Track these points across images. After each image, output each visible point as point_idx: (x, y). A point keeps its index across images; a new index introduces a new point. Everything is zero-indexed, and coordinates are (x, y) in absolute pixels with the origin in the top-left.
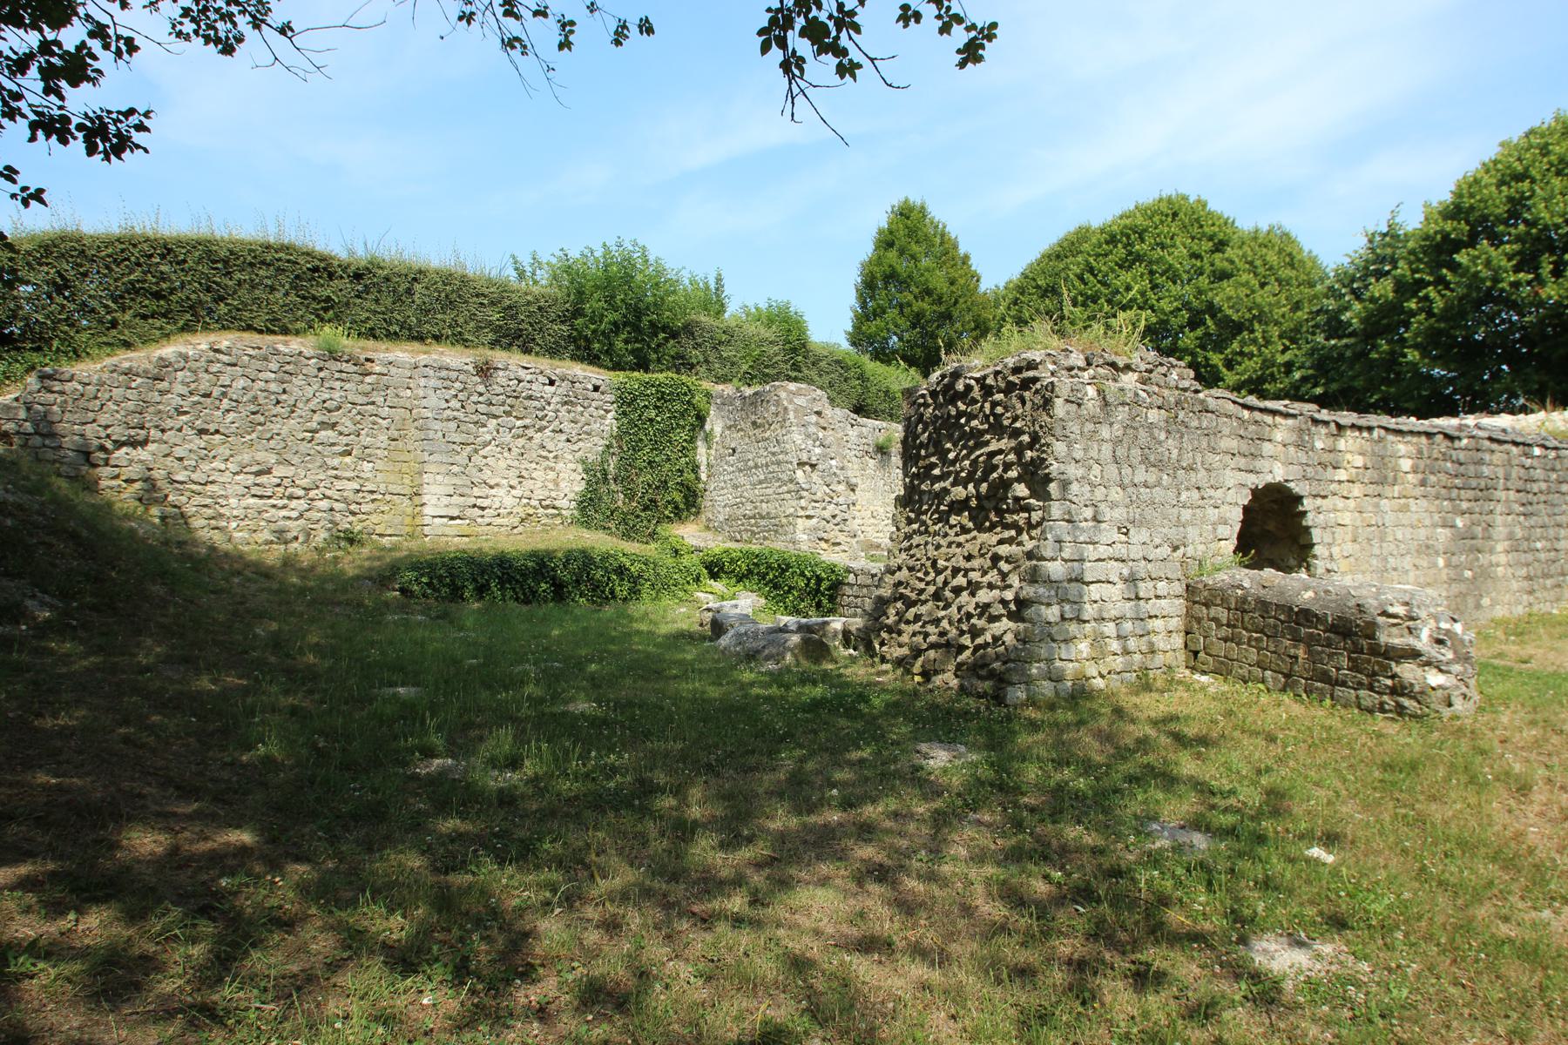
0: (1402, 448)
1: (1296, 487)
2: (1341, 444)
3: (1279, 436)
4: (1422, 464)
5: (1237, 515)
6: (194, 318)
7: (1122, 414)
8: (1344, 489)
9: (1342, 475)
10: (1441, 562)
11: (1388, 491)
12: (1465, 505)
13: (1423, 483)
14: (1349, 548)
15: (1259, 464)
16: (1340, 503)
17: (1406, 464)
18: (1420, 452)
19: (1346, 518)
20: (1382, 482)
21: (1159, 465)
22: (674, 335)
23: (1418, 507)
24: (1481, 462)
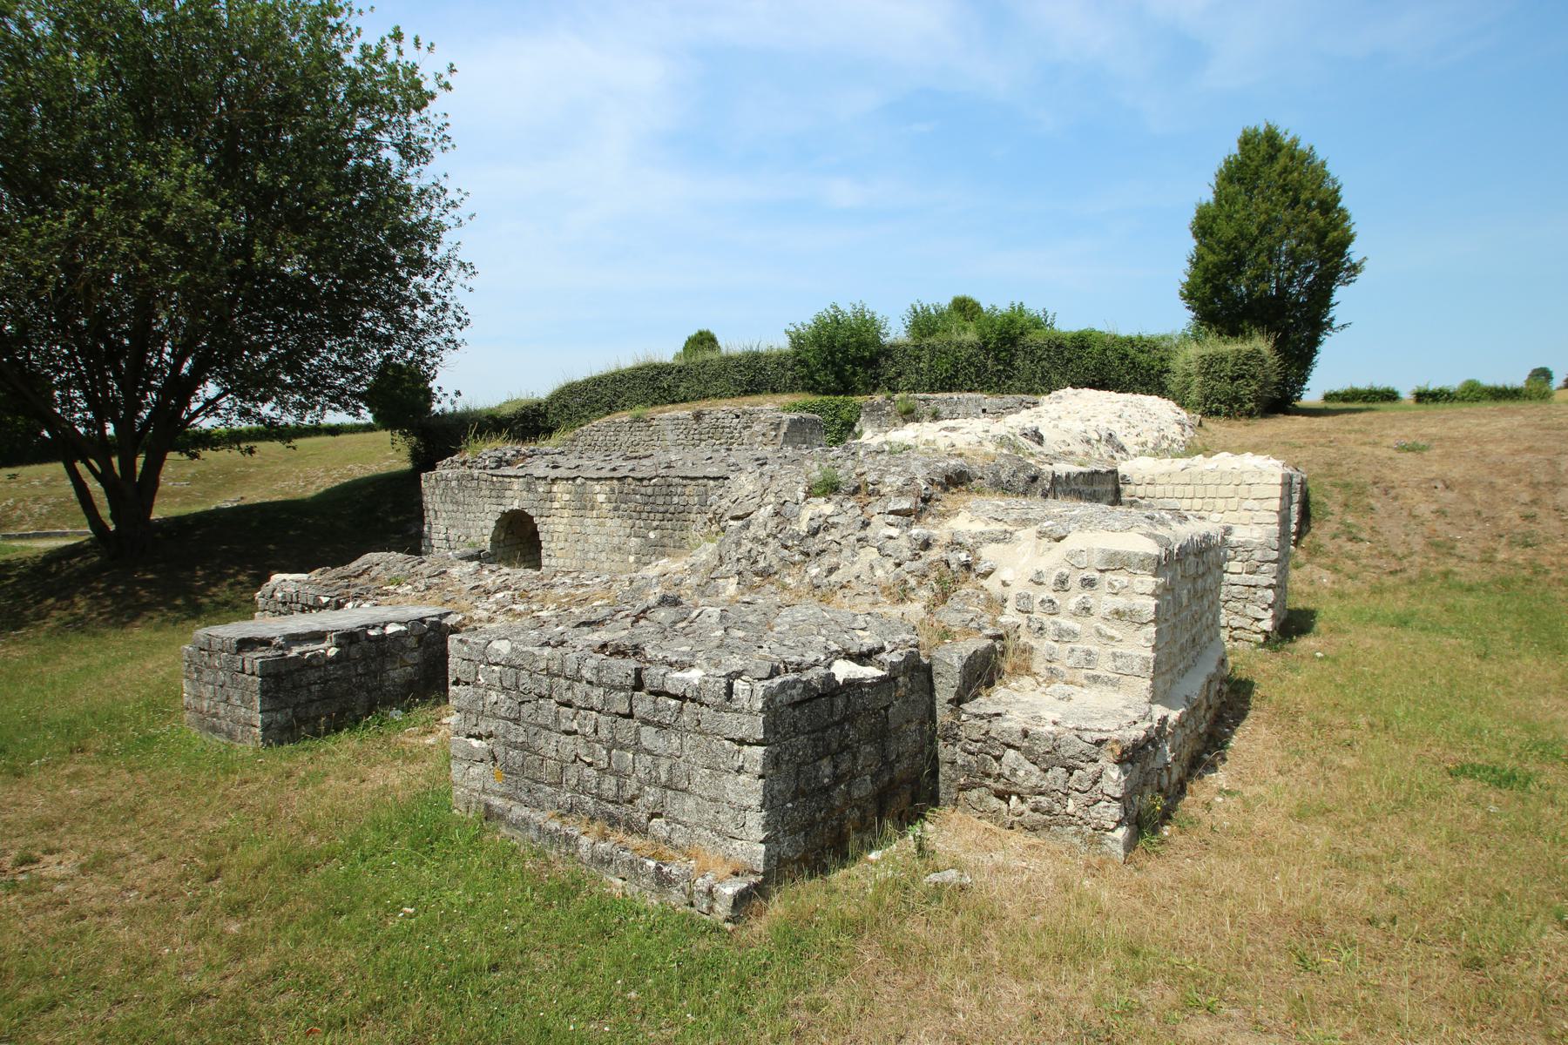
0: (597, 488)
1: (532, 512)
2: (555, 488)
3: (516, 487)
4: (613, 498)
5: (492, 524)
6: (611, 408)
7: (442, 484)
8: (558, 513)
9: (556, 505)
10: (632, 559)
11: (588, 513)
12: (655, 524)
13: (616, 509)
14: (561, 545)
15: (504, 501)
16: (557, 520)
17: (601, 498)
18: (613, 491)
19: (561, 528)
20: (585, 508)
21: (457, 503)
22: (872, 362)
23: (612, 524)
24: (670, 494)
